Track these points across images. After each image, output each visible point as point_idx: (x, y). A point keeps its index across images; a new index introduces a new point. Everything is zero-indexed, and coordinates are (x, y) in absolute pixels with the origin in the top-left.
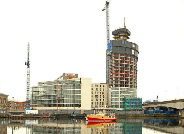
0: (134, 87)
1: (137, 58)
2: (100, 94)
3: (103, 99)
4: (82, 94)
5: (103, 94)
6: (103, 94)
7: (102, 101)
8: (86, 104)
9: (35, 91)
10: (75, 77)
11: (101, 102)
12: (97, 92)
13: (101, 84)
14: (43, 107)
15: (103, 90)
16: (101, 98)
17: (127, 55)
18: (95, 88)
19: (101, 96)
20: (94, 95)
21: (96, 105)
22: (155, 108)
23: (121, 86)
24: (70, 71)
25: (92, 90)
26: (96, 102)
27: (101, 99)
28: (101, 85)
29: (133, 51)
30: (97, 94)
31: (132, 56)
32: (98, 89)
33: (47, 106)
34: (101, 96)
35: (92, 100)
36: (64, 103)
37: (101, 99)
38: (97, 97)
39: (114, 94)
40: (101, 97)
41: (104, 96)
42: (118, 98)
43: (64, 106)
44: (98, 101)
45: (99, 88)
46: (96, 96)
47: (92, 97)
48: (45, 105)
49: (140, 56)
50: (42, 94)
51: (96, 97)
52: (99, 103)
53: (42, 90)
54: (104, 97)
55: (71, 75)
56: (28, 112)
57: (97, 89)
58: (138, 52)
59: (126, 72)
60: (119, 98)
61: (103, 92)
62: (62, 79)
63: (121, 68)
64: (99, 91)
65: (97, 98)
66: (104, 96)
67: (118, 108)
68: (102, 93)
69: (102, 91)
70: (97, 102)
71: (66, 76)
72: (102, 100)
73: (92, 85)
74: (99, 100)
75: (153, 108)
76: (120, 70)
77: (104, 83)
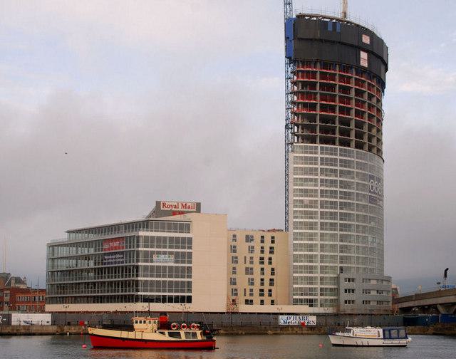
1: (382, 84)
4: (195, 250)
5: (270, 263)
6: (270, 263)
7: (267, 287)
8: (209, 295)
13: (263, 234)
15: (272, 250)
17: (346, 68)
18: (243, 248)
19: (262, 269)
20: (241, 267)
21: (248, 298)
22: (440, 308)
23: (324, 141)
27: (262, 280)
28: (263, 237)
29: (364, 55)
30: (251, 262)
31: (361, 71)
34: (262, 269)
36: (137, 291)
37: (262, 280)
38: (252, 273)
39: (301, 209)
41: (273, 269)
43: (136, 299)
44: (252, 284)
45: (257, 244)
46: (247, 269)
47: (234, 273)
49: (390, 77)
51: (247, 273)
52: (256, 292)
56: (18, 318)
57: (251, 249)
59: (343, 122)
63: (323, 98)
64: (257, 255)
65: (251, 276)
67: (316, 306)
68: (266, 261)
69: (267, 255)
70: (251, 287)
72: (267, 282)
73: (234, 236)
74: (257, 282)
75: (434, 307)
76: (321, 104)
77: (274, 230)
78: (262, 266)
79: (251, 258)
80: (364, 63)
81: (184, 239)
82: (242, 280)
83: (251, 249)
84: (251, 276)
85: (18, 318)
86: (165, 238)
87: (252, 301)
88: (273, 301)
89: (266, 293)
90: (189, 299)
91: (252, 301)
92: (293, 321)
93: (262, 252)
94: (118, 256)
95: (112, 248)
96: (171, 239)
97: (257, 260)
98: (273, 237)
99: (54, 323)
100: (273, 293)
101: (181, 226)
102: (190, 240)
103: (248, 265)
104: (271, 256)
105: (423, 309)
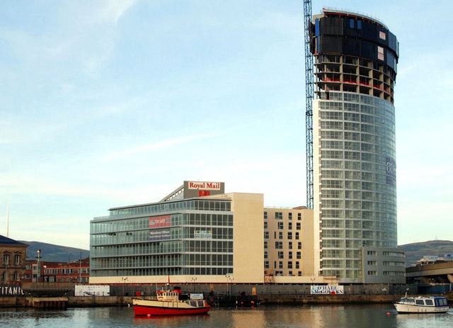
0: (386, 96)
1: (394, 74)
2: (290, 237)
3: (299, 253)
5: (297, 238)
6: (297, 238)
7: (294, 260)
8: (248, 267)
9: (106, 231)
10: (216, 193)
11: (290, 260)
12: (281, 233)
14: (125, 277)
16: (291, 250)
18: (274, 223)
19: (290, 243)
20: (272, 242)
21: (278, 269)
24: (203, 175)
25: (265, 227)
26: (278, 260)
27: (290, 253)
28: (290, 214)
29: (380, 50)
31: (378, 64)
32: (282, 224)
33: (135, 272)
34: (290, 243)
35: (266, 257)
38: (281, 247)
39: (327, 189)
40: (291, 248)
41: (300, 243)
42: (340, 130)
44: (282, 257)
46: (277, 243)
47: (266, 247)
48: (130, 270)
49: (402, 69)
50: (123, 240)
51: (277, 247)
52: (285, 264)
53: (123, 228)
54: (300, 248)
55: (206, 186)
56: (80, 290)
58: (397, 58)
60: (343, 121)
61: (297, 234)
62: (180, 196)
64: (286, 231)
65: (280, 250)
66: (300, 243)
68: (294, 236)
70: (281, 260)
71: (192, 188)
73: (265, 213)
74: (286, 255)
77: (300, 208)
78: (290, 240)
79: (281, 233)
80: (381, 57)
81: (225, 216)
82: (274, 252)
83: (281, 225)
84: (280, 250)
85: (80, 290)
86: (209, 215)
87: (281, 272)
88: (300, 273)
89: (294, 265)
90: (231, 271)
91: (281, 272)
92: (323, 290)
93: (290, 228)
94: (164, 232)
95: (158, 225)
96: (214, 216)
97: (285, 235)
98: (299, 214)
99: (112, 293)
100: (300, 265)
101: (223, 206)
102: (231, 217)
103: (278, 240)
104: (298, 231)
105: (437, 278)
